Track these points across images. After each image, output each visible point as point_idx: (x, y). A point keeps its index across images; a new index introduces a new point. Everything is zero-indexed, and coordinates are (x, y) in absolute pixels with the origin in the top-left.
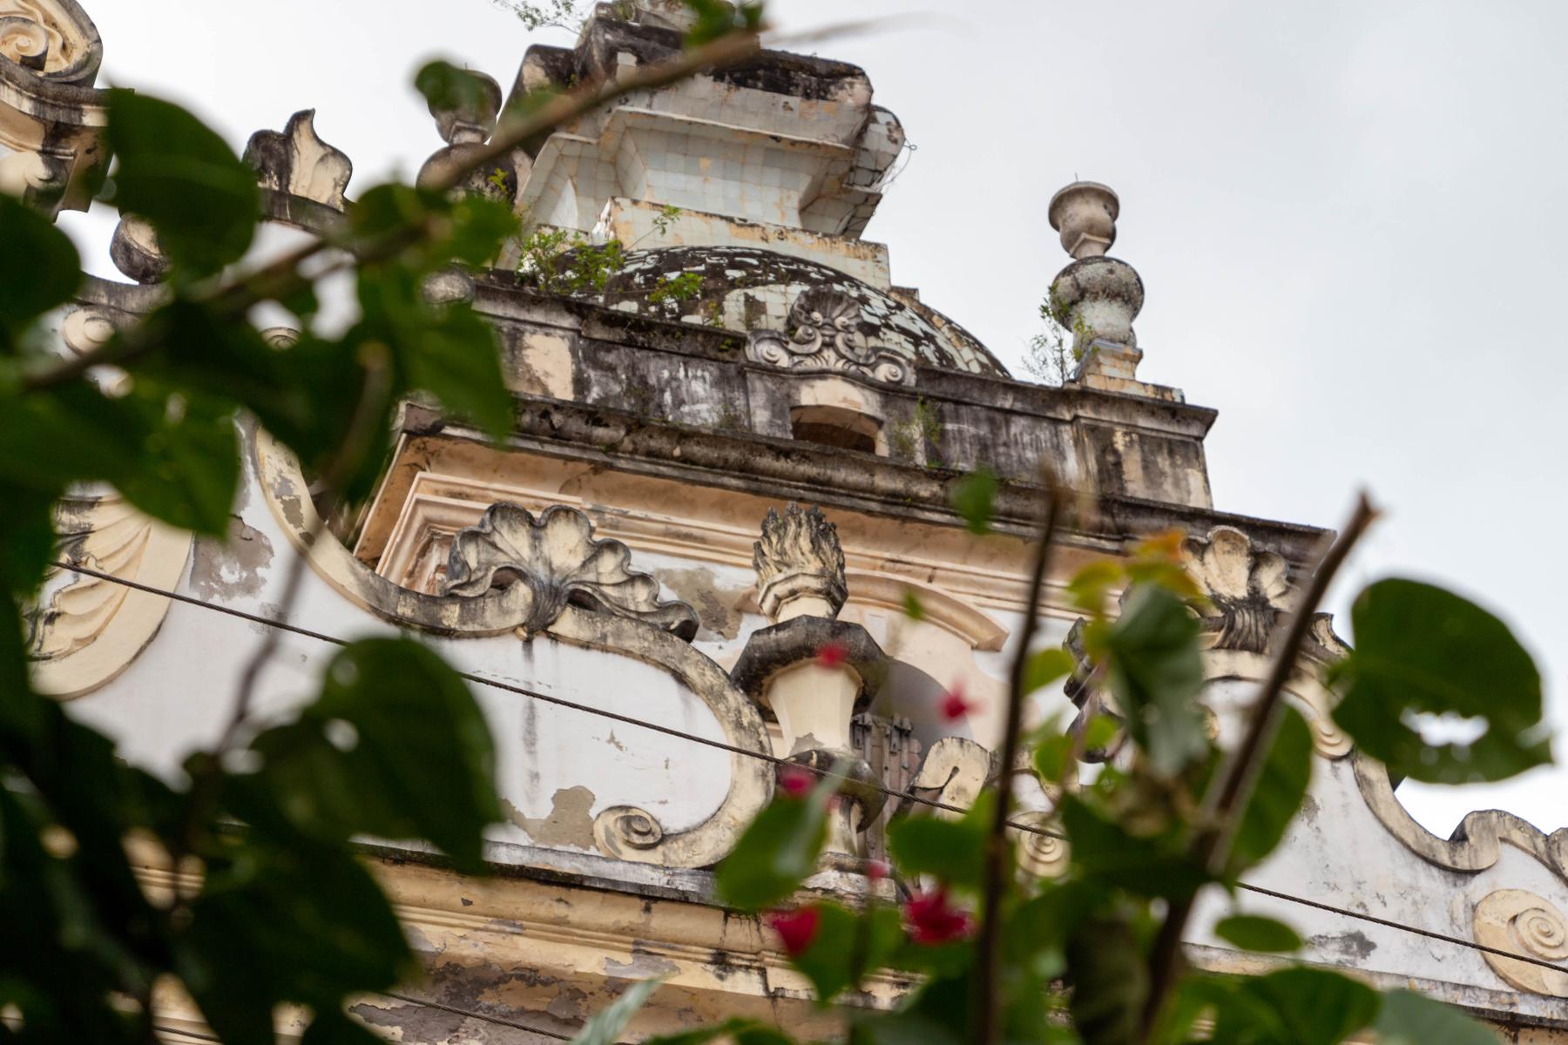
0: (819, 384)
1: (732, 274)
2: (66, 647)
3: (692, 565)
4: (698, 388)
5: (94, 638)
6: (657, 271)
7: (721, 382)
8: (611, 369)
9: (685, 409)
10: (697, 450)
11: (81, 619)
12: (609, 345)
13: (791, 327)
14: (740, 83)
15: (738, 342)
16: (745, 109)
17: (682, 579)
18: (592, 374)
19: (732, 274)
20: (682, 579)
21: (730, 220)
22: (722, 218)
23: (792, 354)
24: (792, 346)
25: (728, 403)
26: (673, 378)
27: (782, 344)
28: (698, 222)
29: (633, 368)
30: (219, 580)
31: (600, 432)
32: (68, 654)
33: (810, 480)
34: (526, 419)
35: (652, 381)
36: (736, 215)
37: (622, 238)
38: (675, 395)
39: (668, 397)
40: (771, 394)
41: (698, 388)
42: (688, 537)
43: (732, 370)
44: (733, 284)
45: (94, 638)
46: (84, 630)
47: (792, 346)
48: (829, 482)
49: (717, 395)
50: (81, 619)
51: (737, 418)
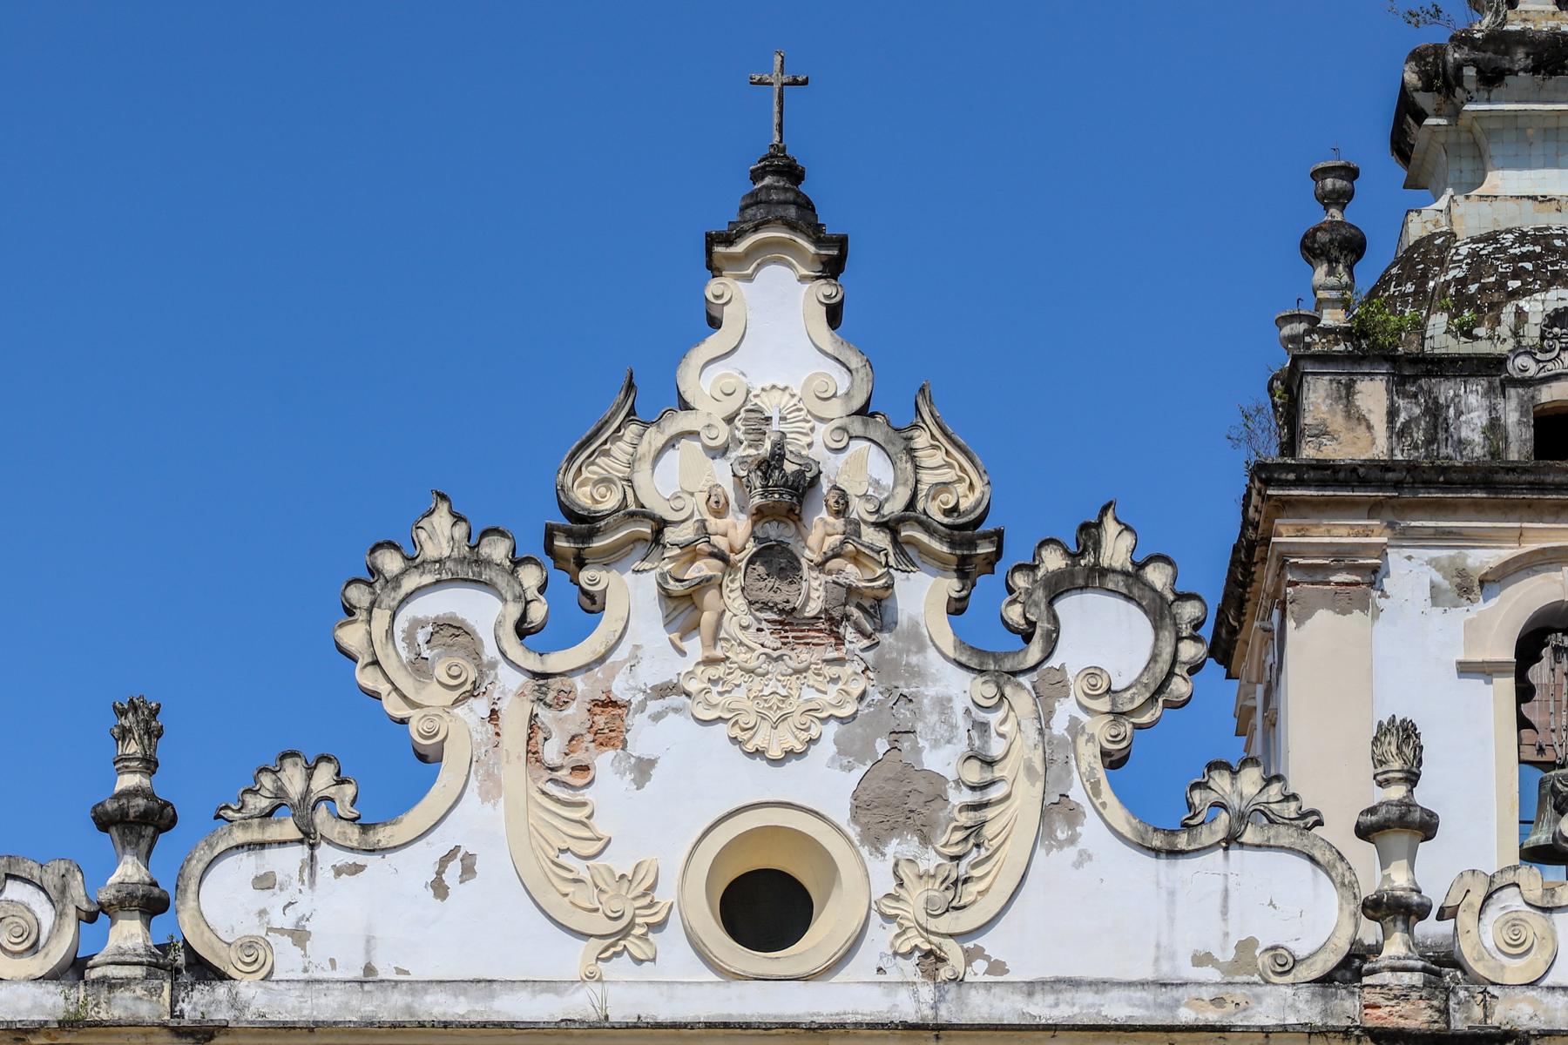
0: (1555, 385)
1: (1514, 284)
2: (971, 898)
3: (1453, 552)
4: (1473, 400)
5: (987, 890)
6: (1462, 282)
7: (1489, 392)
8: (1415, 396)
9: (1463, 418)
10: (1454, 476)
11: (981, 878)
12: (1415, 378)
13: (1543, 338)
14: (1553, 73)
15: (1498, 363)
16: (1556, 90)
17: (1445, 563)
18: (1401, 403)
19: (1514, 284)
20: (1445, 563)
21: (1534, 198)
22: (1529, 197)
23: (1538, 361)
24: (1539, 356)
25: (1492, 408)
26: (1456, 395)
27: (1531, 354)
28: (1512, 205)
29: (1430, 391)
30: (1056, 839)
31: (1390, 475)
32: (974, 902)
33: (1530, 483)
34: (1341, 475)
35: (1442, 400)
36: (1539, 192)
37: (1456, 229)
38: (1456, 409)
39: (1452, 411)
40: (1520, 397)
41: (1473, 400)
42: (1450, 533)
43: (1497, 381)
44: (1514, 294)
45: (987, 890)
46: (982, 886)
47: (1539, 356)
48: (1543, 483)
49: (1485, 402)
50: (981, 878)
51: (1498, 419)
